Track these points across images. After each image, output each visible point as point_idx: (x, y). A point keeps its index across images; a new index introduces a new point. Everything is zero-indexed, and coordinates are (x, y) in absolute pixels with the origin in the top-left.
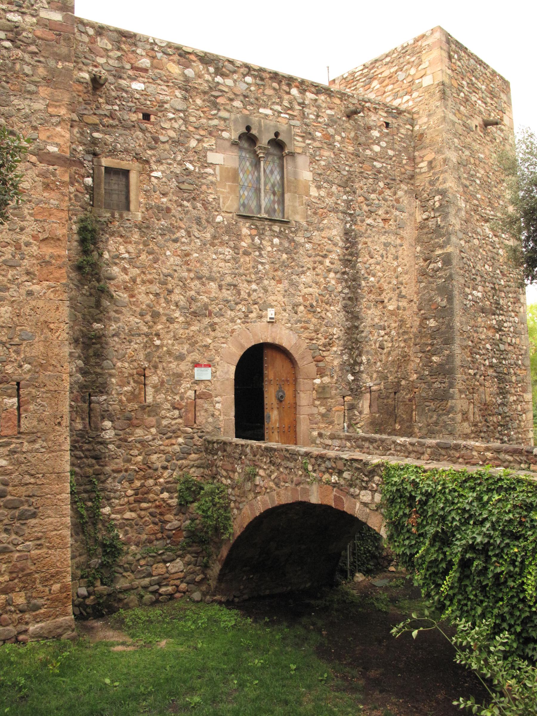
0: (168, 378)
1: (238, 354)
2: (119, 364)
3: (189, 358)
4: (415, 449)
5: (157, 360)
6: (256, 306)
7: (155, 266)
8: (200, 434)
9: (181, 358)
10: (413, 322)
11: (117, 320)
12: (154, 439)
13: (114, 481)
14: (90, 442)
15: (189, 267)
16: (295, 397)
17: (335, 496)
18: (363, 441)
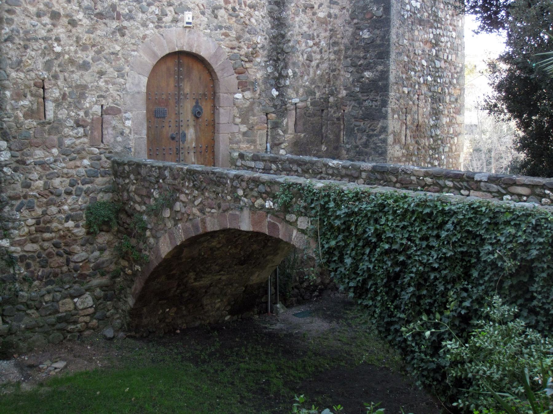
0: (70, 90)
1: (150, 62)
2: (13, 74)
3: (95, 68)
4: (349, 173)
5: (58, 69)
6: (171, 8)
8: (108, 155)
9: (85, 66)
10: (345, 32)
11: (10, 22)
12: (55, 161)
13: (12, 210)
16: (214, 113)
17: (269, 222)
18: (290, 163)
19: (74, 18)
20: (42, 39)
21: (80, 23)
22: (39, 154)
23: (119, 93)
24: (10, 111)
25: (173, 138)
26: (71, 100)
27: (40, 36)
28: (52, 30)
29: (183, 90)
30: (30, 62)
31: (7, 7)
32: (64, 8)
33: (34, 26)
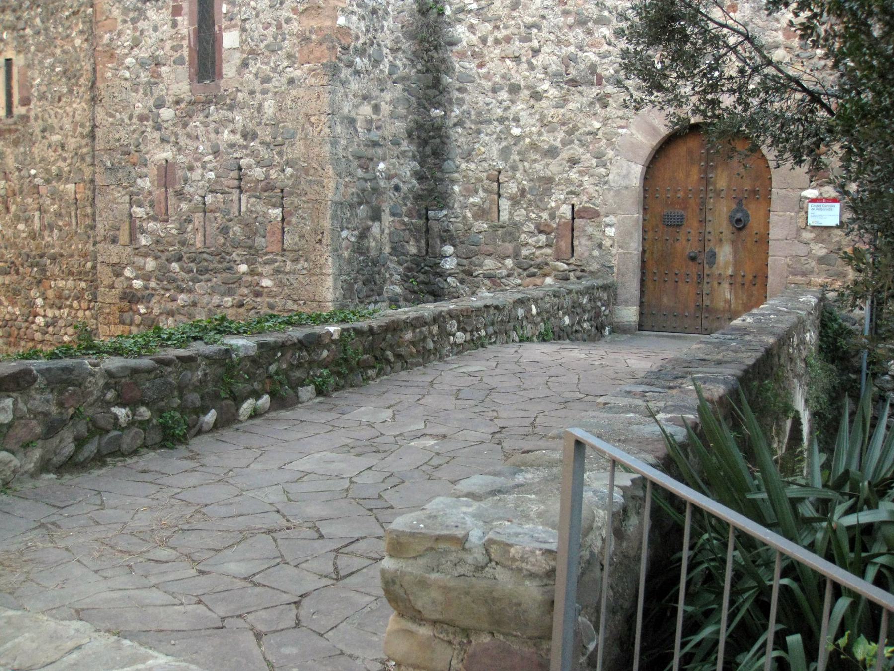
2: (464, 166)
3: (565, 154)
7: (514, 14)
8: (578, 274)
9: (552, 152)
11: (460, 102)
12: (509, 276)
14: (425, 273)
15: (567, 7)
19: (539, 89)
20: (497, 120)
21: (545, 95)
22: (489, 264)
23: (597, 188)
24: (459, 210)
25: (693, 259)
26: (532, 198)
27: (495, 117)
28: (509, 108)
29: (714, 184)
30: (483, 149)
31: (458, 85)
32: (526, 78)
33: (488, 105)
